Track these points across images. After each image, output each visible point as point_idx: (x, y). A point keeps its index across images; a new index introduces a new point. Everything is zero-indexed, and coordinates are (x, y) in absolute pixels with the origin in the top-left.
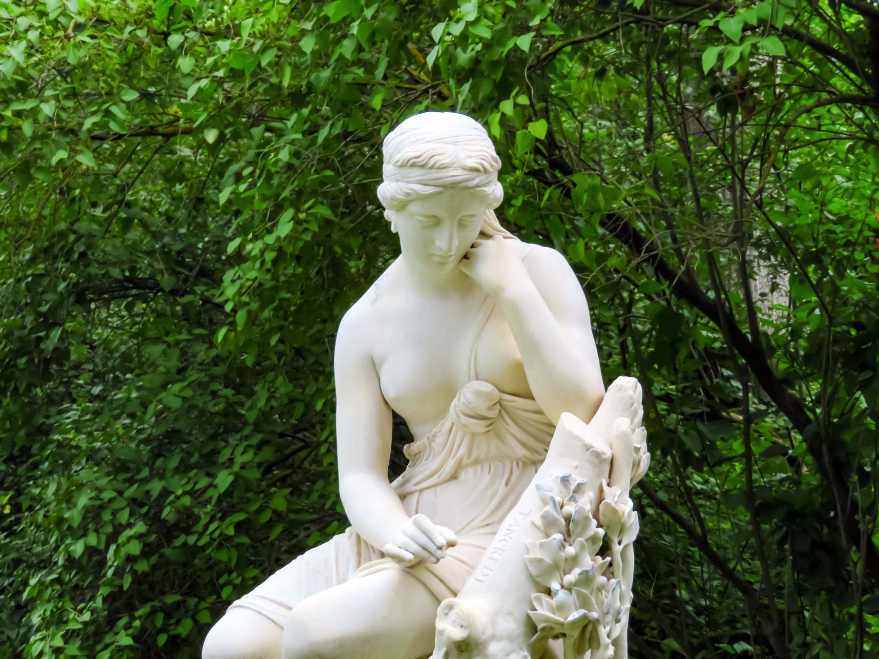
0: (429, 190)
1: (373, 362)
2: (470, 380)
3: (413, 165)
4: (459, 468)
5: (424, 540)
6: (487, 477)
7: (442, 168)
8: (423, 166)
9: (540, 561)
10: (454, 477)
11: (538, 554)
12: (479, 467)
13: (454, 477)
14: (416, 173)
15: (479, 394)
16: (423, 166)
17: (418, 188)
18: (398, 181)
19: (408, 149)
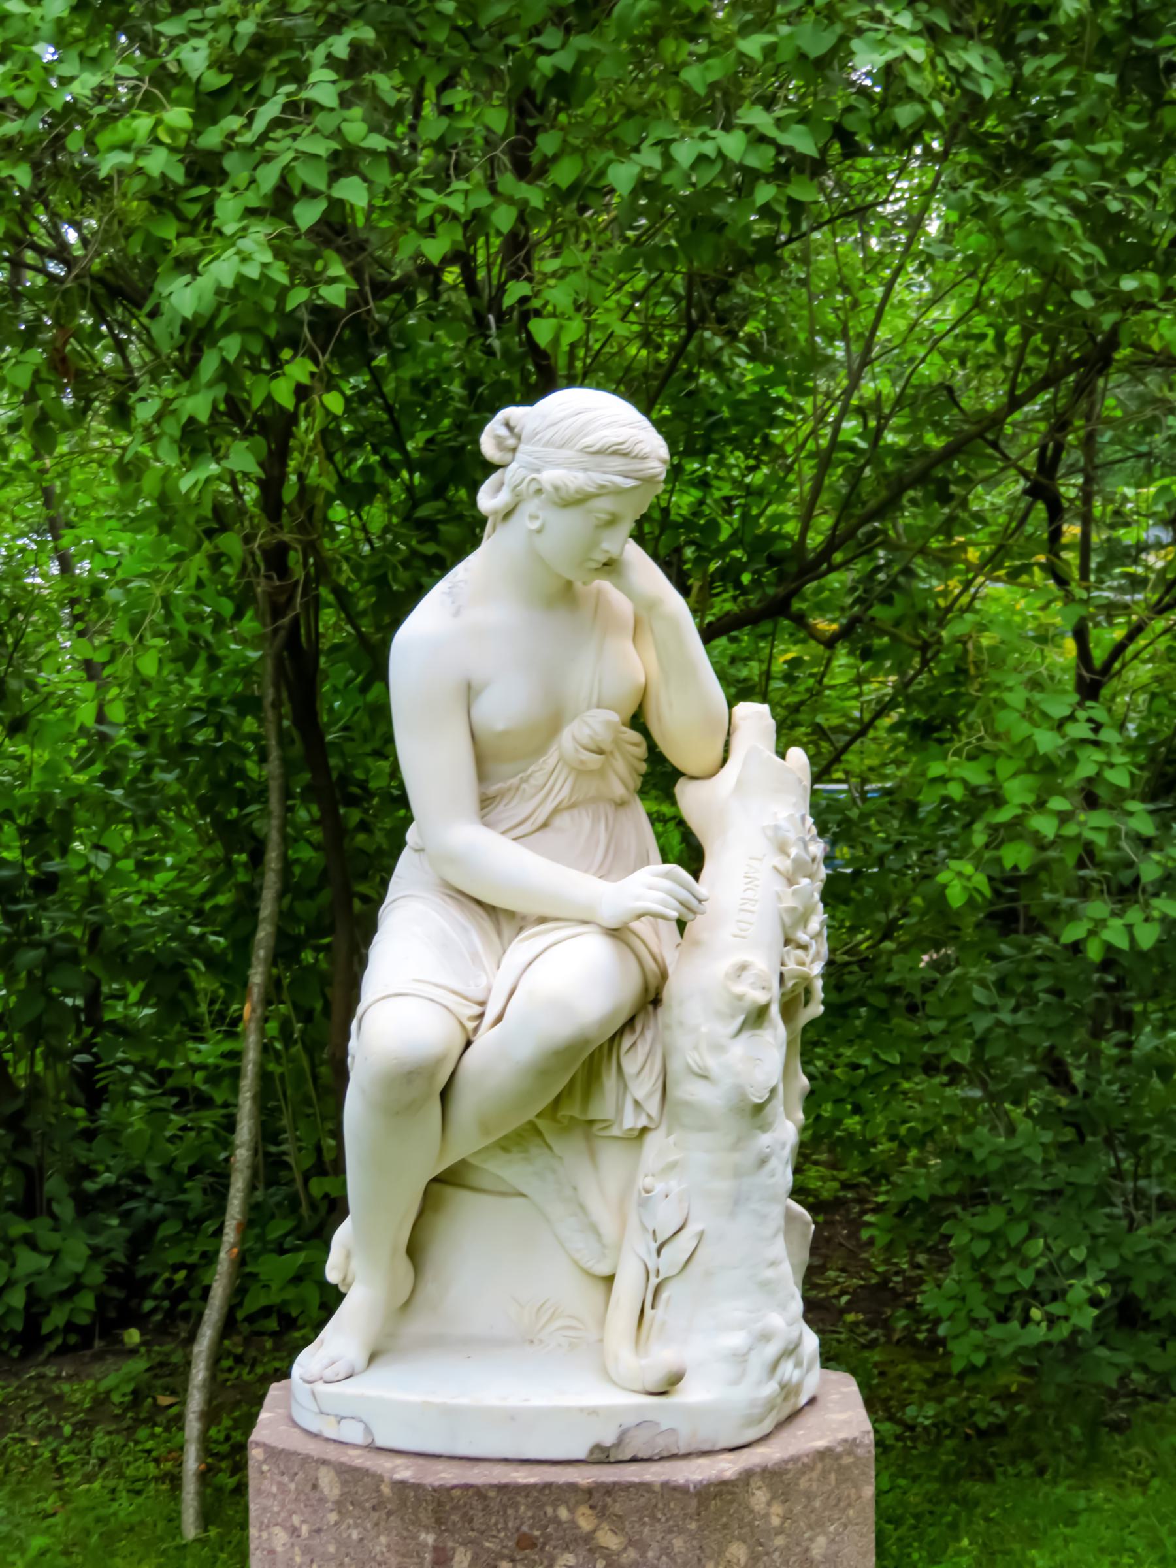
0: (630, 483)
1: (469, 687)
2: (589, 708)
3: (615, 453)
4: (556, 811)
5: (684, 895)
6: (587, 823)
7: (644, 458)
8: (626, 455)
9: (794, 909)
10: (545, 825)
11: (790, 902)
12: (575, 812)
13: (545, 825)
14: (617, 463)
15: (608, 724)
16: (626, 455)
17: (619, 480)
18: (585, 470)
19: (606, 432)
